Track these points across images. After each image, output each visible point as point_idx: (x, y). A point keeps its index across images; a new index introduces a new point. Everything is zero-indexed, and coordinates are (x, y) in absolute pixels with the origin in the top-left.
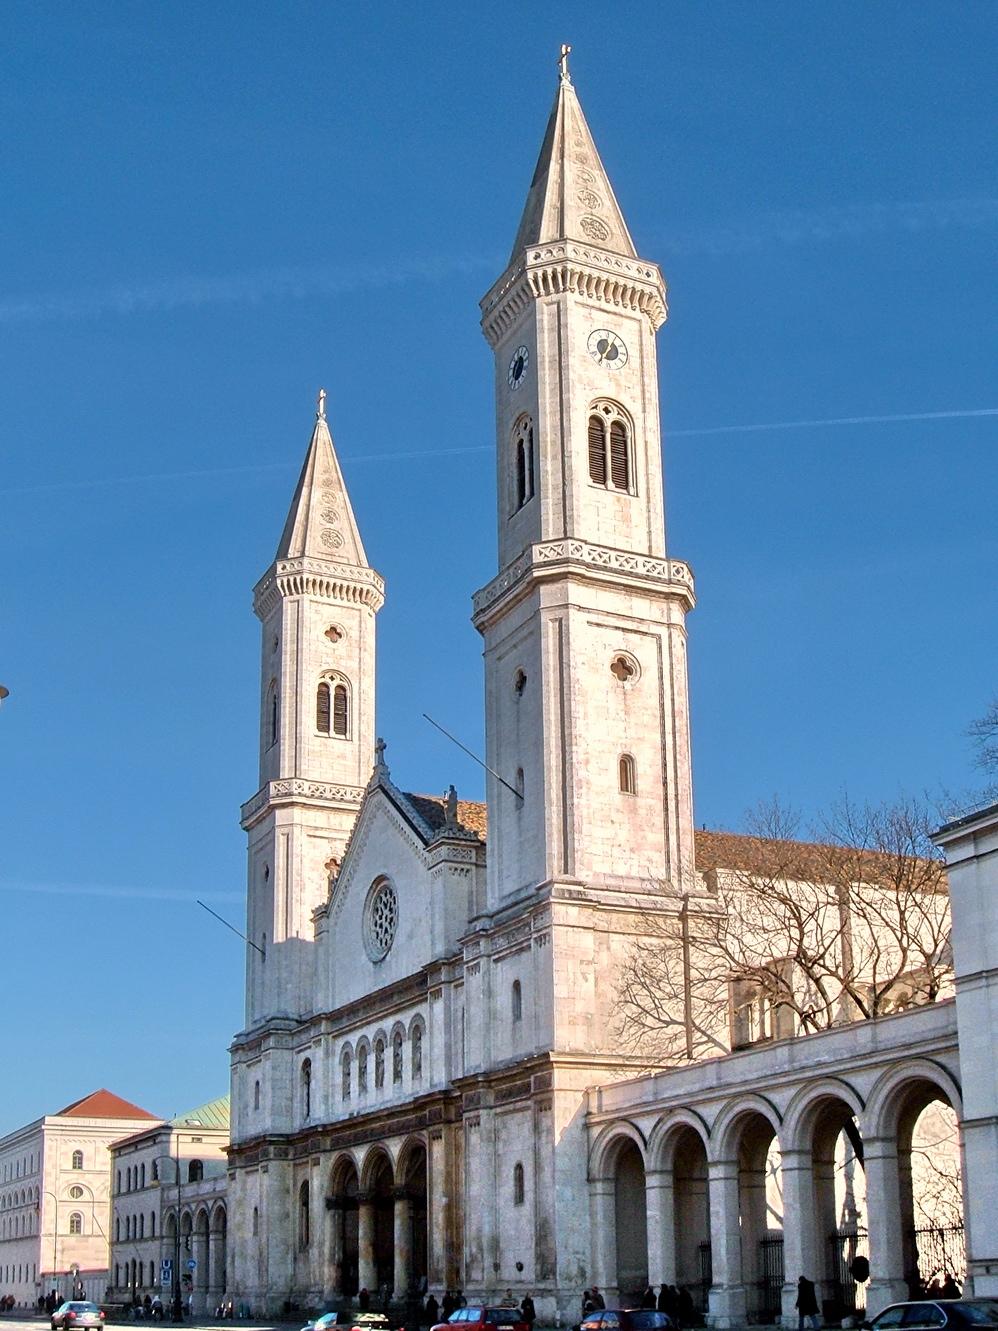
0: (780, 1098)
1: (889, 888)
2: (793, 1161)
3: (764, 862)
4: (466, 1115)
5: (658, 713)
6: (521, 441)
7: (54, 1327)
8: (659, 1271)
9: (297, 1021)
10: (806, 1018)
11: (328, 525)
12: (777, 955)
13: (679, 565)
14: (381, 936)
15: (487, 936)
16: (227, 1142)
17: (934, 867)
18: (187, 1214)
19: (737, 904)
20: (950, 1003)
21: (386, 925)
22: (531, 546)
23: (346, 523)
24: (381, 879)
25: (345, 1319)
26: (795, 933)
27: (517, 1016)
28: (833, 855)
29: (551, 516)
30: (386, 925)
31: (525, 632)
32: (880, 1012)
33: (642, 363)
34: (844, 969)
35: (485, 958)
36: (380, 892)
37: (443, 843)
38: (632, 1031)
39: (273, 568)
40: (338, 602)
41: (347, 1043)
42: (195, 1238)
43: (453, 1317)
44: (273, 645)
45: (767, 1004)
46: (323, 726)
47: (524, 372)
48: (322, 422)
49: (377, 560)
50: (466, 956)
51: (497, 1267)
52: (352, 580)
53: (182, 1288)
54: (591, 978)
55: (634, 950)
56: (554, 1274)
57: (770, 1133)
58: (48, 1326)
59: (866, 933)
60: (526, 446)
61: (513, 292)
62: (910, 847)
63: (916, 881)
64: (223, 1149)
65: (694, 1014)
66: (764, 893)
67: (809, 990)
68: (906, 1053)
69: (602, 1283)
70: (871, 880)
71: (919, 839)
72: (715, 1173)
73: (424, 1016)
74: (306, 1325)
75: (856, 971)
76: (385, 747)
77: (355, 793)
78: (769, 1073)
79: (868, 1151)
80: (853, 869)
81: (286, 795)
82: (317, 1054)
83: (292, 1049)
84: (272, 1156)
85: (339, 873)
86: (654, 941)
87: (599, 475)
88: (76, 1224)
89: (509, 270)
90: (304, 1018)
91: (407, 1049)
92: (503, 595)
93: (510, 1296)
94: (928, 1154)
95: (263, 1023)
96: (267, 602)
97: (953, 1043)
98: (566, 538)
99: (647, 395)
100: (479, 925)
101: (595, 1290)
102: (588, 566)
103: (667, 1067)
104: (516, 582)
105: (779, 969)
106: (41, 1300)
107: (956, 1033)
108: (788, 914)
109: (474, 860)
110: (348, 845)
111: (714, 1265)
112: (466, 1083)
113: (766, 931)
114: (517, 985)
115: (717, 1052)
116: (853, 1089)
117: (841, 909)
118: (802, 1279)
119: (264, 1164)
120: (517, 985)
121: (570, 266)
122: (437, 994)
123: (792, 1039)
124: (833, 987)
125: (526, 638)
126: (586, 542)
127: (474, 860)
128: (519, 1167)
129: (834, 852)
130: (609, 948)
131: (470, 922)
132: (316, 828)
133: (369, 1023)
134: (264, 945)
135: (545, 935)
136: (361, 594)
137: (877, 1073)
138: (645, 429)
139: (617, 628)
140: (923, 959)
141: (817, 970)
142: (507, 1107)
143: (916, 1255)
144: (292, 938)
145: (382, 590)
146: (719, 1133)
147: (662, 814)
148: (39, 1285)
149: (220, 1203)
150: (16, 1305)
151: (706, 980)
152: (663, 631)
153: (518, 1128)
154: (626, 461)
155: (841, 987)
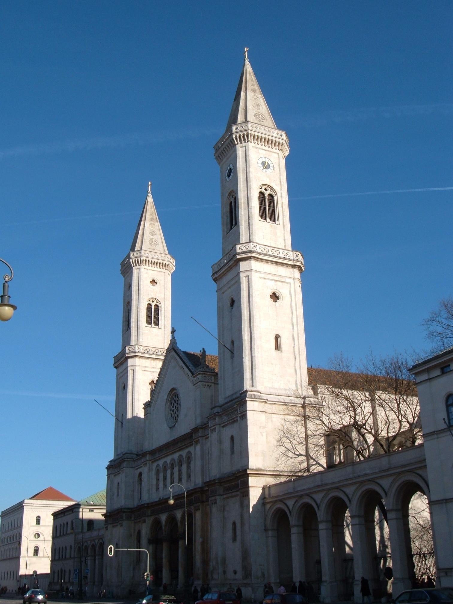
0: (350, 490)
1: (392, 394)
2: (356, 521)
3: (338, 381)
4: (210, 499)
5: (290, 316)
6: (231, 202)
7: (24, 602)
8: (298, 576)
9: (136, 455)
10: (359, 453)
11: (152, 237)
12: (345, 424)
13: (297, 253)
14: (173, 415)
15: (219, 415)
16: (104, 511)
17: (411, 384)
18: (86, 546)
19: (327, 400)
20: (420, 445)
21: (175, 410)
22: (236, 245)
23: (159, 236)
24: (173, 389)
25: (156, 599)
26: (352, 414)
27: (232, 452)
28: (367, 379)
29: (244, 233)
30: (175, 410)
31: (233, 282)
32: (391, 450)
33: (280, 170)
34: (374, 431)
35: (218, 426)
36: (173, 395)
38: (283, 459)
39: (129, 255)
40: (156, 269)
41: (158, 465)
42: (89, 558)
43: (205, 597)
44: (128, 287)
45: (341, 447)
46: (149, 322)
47: (232, 174)
48: (150, 195)
49: (172, 251)
50: (210, 425)
51: (225, 572)
52: (162, 260)
53: (83, 583)
54: (264, 434)
55: (283, 422)
56: (251, 576)
57: (346, 508)
58: (22, 601)
59: (383, 414)
60: (233, 204)
61: (227, 142)
62: (400, 375)
63: (404, 390)
64: (103, 515)
65: (310, 451)
66: (338, 395)
67: (359, 440)
68: (403, 469)
69: (272, 580)
70: (384, 389)
71: (404, 371)
72: (322, 526)
73: (192, 452)
74: (139, 601)
75: (380, 431)
76: (175, 331)
77: (162, 352)
78: (344, 479)
79: (389, 516)
80: (376, 385)
81: (133, 352)
82: (145, 470)
83: (134, 467)
84: (124, 518)
85: (155, 387)
86: (292, 417)
87: (263, 216)
88: (36, 552)
89: (225, 134)
90: (139, 453)
91: (184, 467)
92: (224, 266)
93: (231, 586)
94: (416, 517)
95: (121, 455)
96: (126, 269)
97: (424, 464)
98: (250, 242)
99: (282, 183)
100: (215, 410)
101: (269, 584)
102: (259, 254)
103: (299, 476)
104: (230, 261)
105: (346, 430)
106: (19, 589)
107: (425, 460)
108: (349, 405)
109: (213, 381)
110: (159, 375)
111: (323, 571)
112: (210, 483)
113: (340, 413)
114: (232, 438)
115: (320, 469)
116: (381, 486)
117: (371, 403)
118: (363, 578)
119: (121, 522)
120: (232, 438)
121: (250, 132)
122: (197, 442)
123: (353, 463)
124: (370, 439)
125: (234, 284)
126: (258, 244)
127: (213, 381)
128: (234, 524)
129: (367, 377)
130: (272, 421)
131: (212, 409)
132: (146, 367)
133: (167, 456)
134: (122, 420)
135: (244, 415)
136: (165, 266)
137: (391, 479)
138: (281, 197)
139: (272, 280)
140: (408, 425)
141: (363, 431)
142: (229, 495)
143: (413, 566)
144: (135, 417)
145: (174, 264)
146: (323, 507)
147: (293, 360)
148: (18, 581)
149: (101, 541)
150: (8, 591)
151: (315, 435)
152: (291, 281)
153: (234, 504)
154: (274, 210)
155: (373, 439)
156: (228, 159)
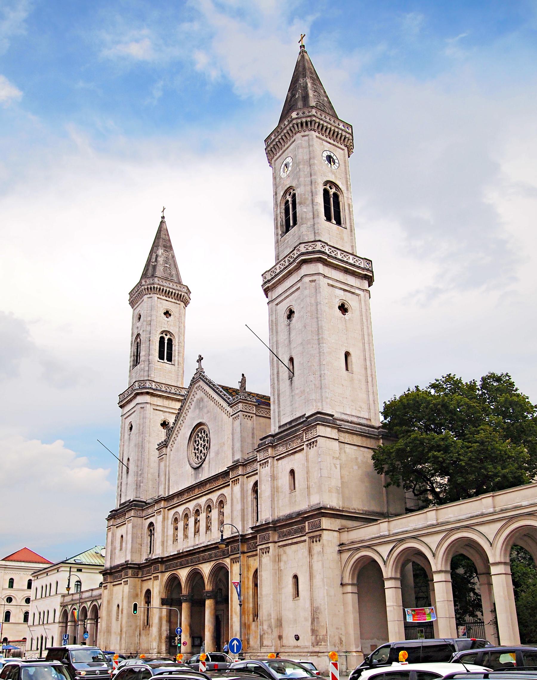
46: (161, 357)
91: (215, 513)
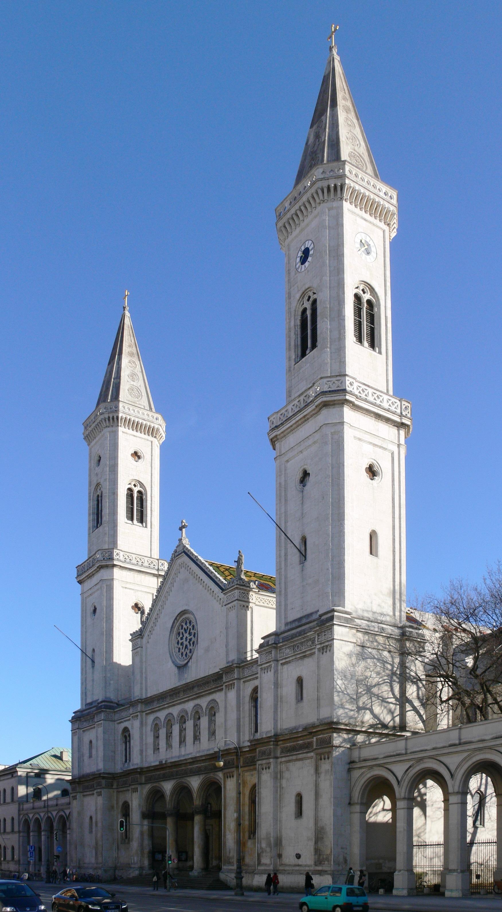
6: (305, 310)
37: (237, 588)
47: (310, 259)
91: (204, 722)
156: (302, 230)
